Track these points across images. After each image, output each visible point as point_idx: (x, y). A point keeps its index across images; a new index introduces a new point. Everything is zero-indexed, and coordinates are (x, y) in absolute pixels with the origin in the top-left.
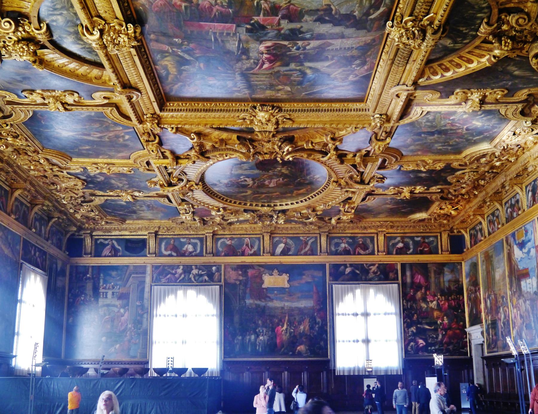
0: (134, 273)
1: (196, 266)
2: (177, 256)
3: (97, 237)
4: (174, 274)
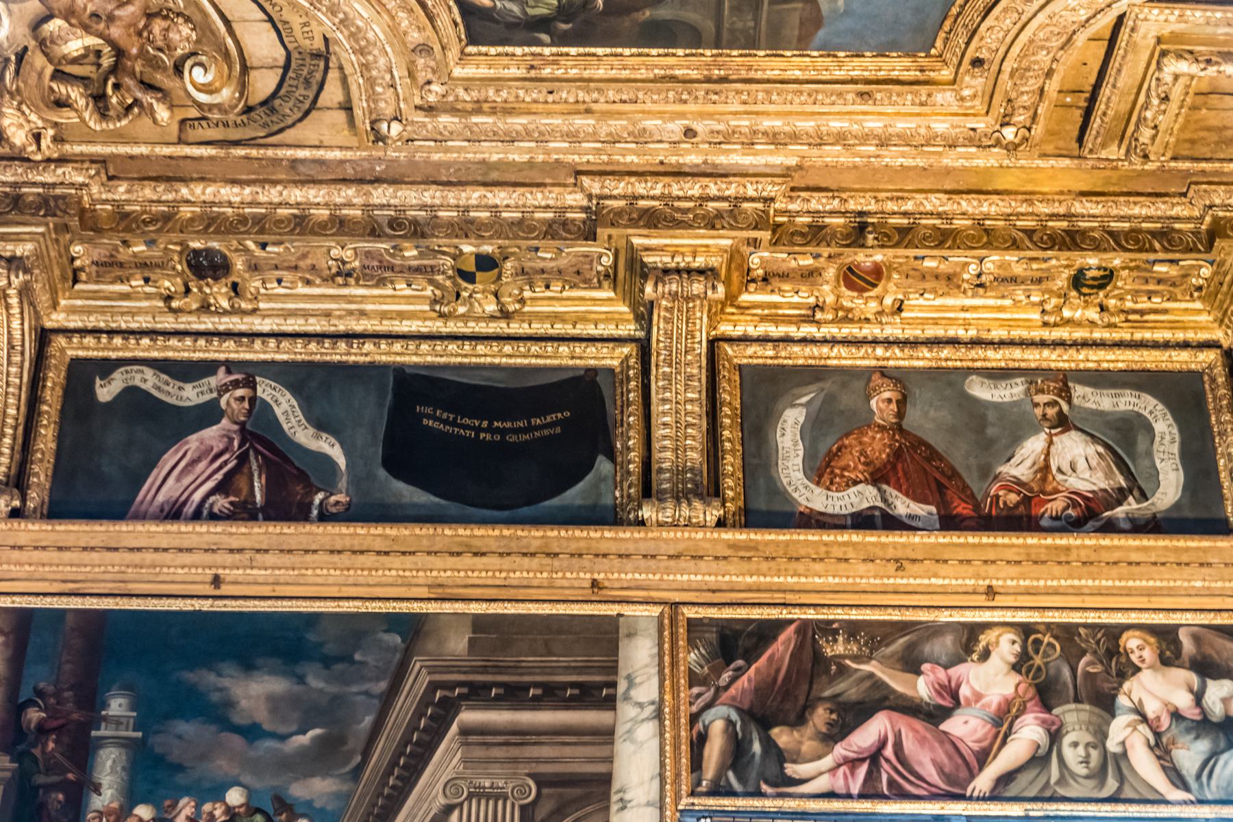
0: (477, 694)
1: (1166, 636)
2: (949, 523)
3: (90, 349)
4: (933, 715)
